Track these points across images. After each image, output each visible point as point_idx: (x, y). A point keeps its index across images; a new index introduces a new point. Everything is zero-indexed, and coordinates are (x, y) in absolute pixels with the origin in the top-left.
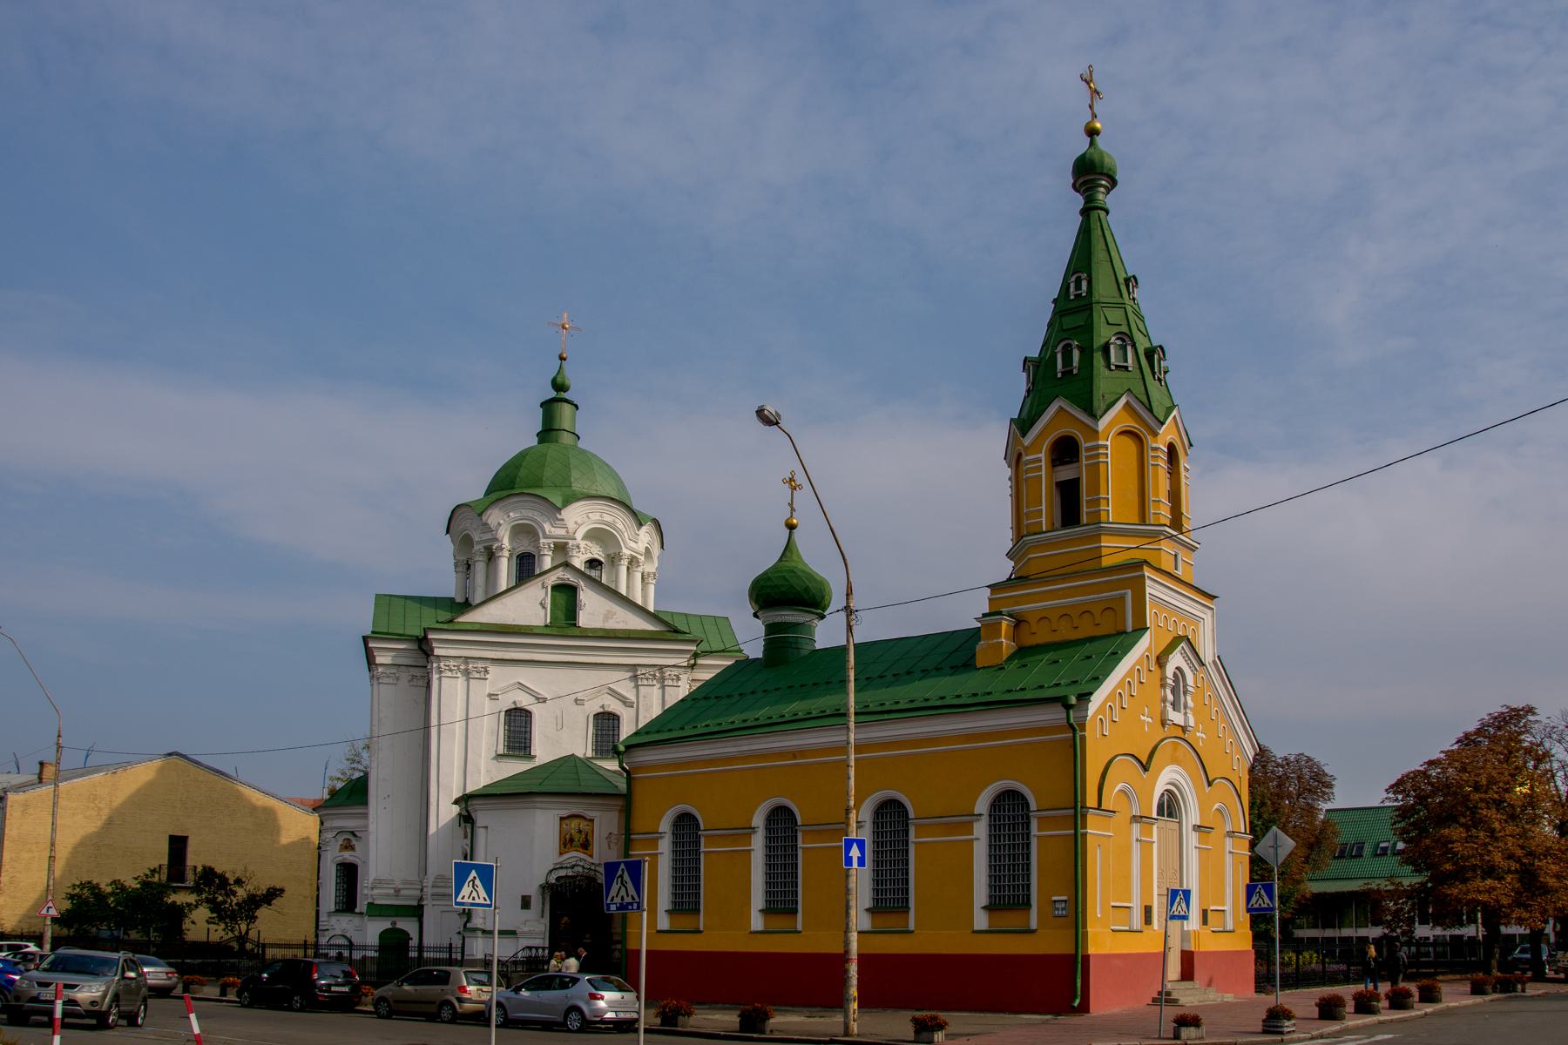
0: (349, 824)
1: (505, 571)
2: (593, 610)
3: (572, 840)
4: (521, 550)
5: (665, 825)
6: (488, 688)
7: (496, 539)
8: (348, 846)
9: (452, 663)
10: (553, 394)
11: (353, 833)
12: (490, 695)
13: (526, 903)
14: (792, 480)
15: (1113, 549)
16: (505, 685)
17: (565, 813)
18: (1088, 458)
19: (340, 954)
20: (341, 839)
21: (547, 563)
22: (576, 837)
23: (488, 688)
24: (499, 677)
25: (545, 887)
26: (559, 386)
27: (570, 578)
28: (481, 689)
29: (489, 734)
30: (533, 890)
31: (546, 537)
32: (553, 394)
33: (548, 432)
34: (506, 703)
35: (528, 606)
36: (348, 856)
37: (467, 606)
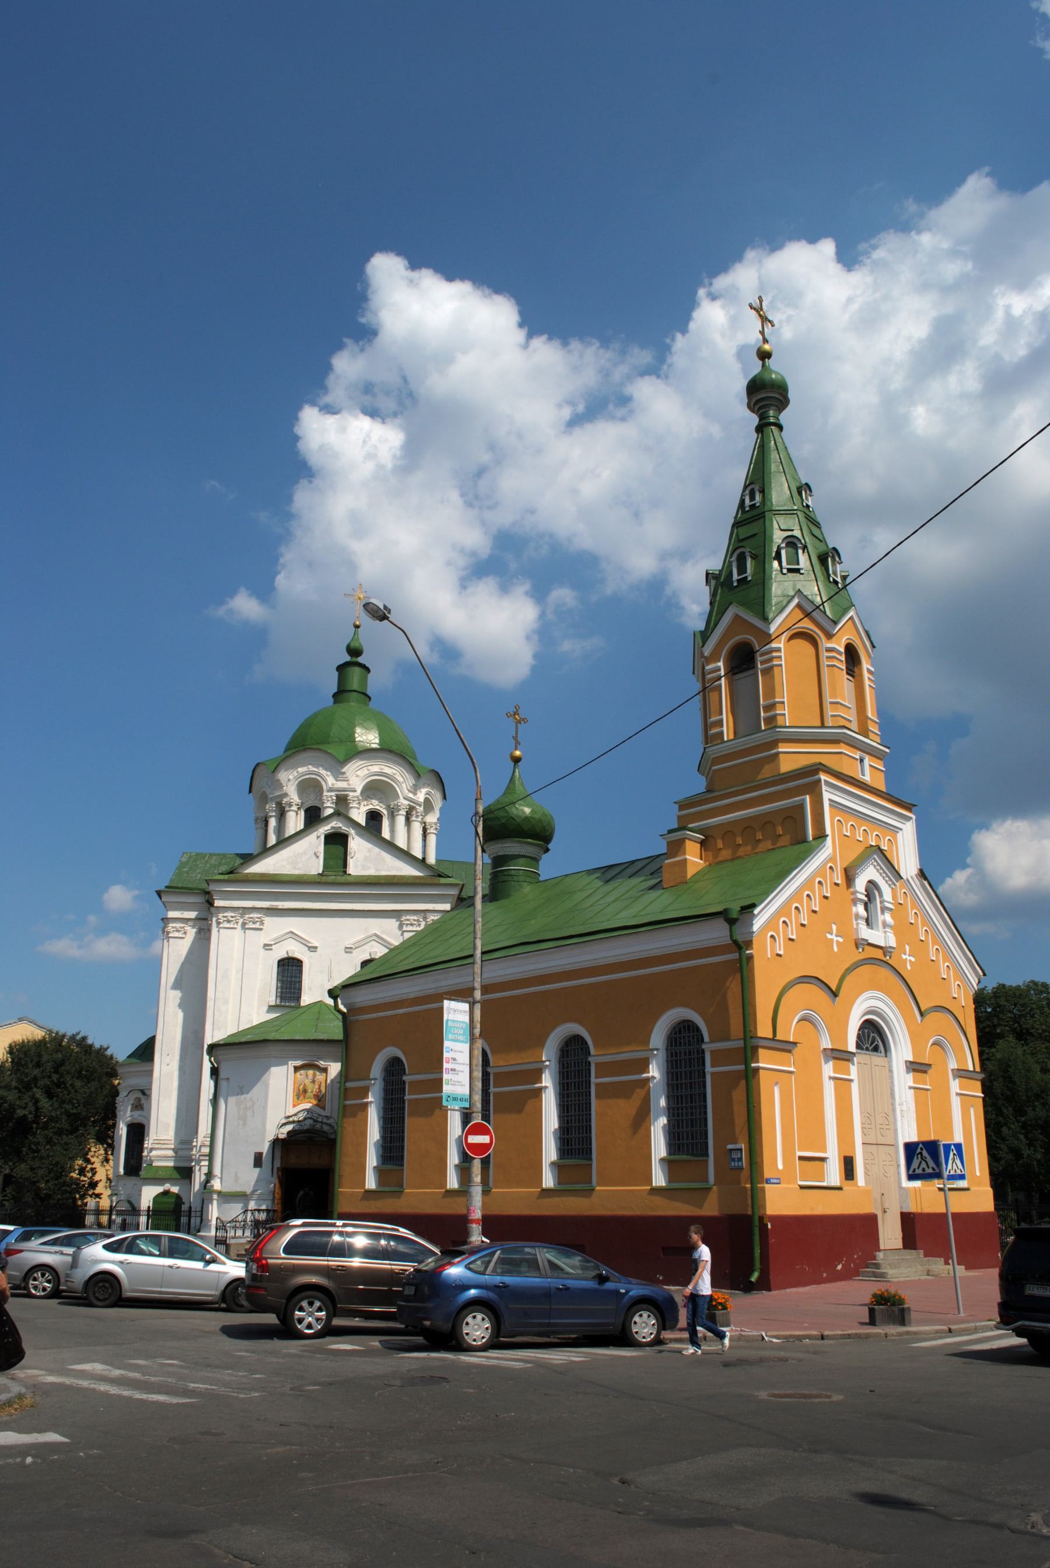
1: (295, 821)
2: (364, 858)
3: (305, 1091)
4: (308, 805)
5: (377, 1070)
6: (264, 938)
7: (286, 795)
9: (229, 914)
10: (348, 658)
12: (265, 945)
13: (258, 1160)
14: (515, 714)
15: (791, 758)
16: (283, 933)
17: (299, 1063)
18: (762, 663)
19: (124, 1220)
23: (264, 938)
24: (275, 926)
26: (354, 652)
27: (344, 828)
30: (265, 1148)
31: (330, 790)
32: (348, 658)
34: (281, 952)
35: (305, 856)
37: (248, 858)
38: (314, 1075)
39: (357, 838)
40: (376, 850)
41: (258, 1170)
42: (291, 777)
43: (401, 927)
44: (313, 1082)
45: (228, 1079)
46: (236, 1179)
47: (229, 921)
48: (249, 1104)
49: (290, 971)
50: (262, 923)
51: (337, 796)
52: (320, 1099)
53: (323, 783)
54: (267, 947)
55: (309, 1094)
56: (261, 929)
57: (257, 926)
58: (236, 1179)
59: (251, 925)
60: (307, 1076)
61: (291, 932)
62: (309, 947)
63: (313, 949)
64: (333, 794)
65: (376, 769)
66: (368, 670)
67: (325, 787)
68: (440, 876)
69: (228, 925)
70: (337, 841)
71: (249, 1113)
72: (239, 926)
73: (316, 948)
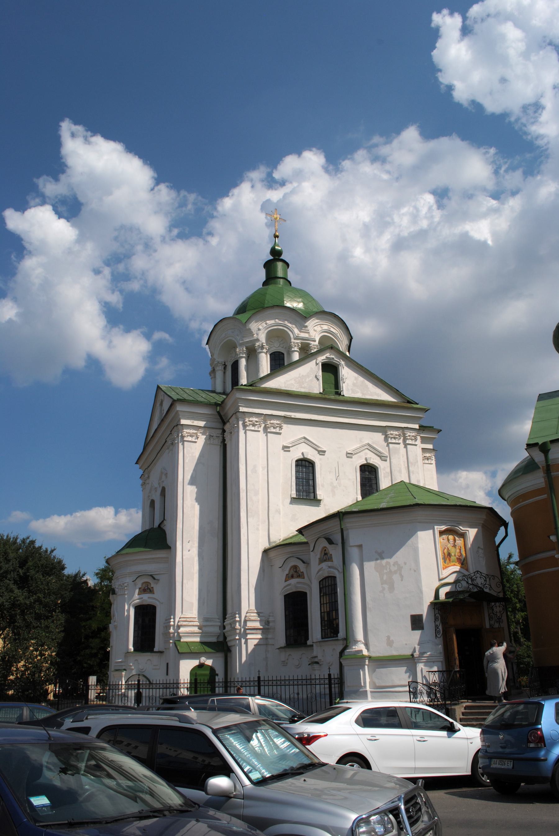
0: (150, 568)
2: (353, 384)
3: (449, 554)
4: (274, 350)
7: (258, 340)
8: (146, 589)
9: (254, 419)
11: (151, 576)
17: (443, 528)
20: (139, 583)
21: (296, 357)
22: (452, 551)
24: (292, 433)
25: (437, 606)
28: (276, 442)
29: (285, 479)
30: (424, 610)
33: (271, 278)
35: (305, 378)
36: (147, 599)
38: (455, 540)
39: (345, 367)
40: (361, 379)
41: (418, 633)
42: (261, 327)
43: (386, 439)
44: (455, 546)
45: (360, 546)
46: (390, 643)
47: (254, 425)
48: (394, 569)
49: (305, 468)
50: (281, 428)
51: (301, 343)
52: (463, 563)
53: (290, 333)
54: (286, 448)
55: (453, 558)
56: (280, 434)
57: (277, 430)
58: (390, 643)
59: (272, 430)
60: (448, 540)
61: (305, 438)
62: (319, 452)
63: (322, 452)
64: (299, 341)
65: (325, 327)
66: (288, 265)
67: (292, 336)
68: (409, 402)
69: (253, 428)
70: (330, 369)
71: (396, 577)
72: (261, 429)
73: (324, 452)
